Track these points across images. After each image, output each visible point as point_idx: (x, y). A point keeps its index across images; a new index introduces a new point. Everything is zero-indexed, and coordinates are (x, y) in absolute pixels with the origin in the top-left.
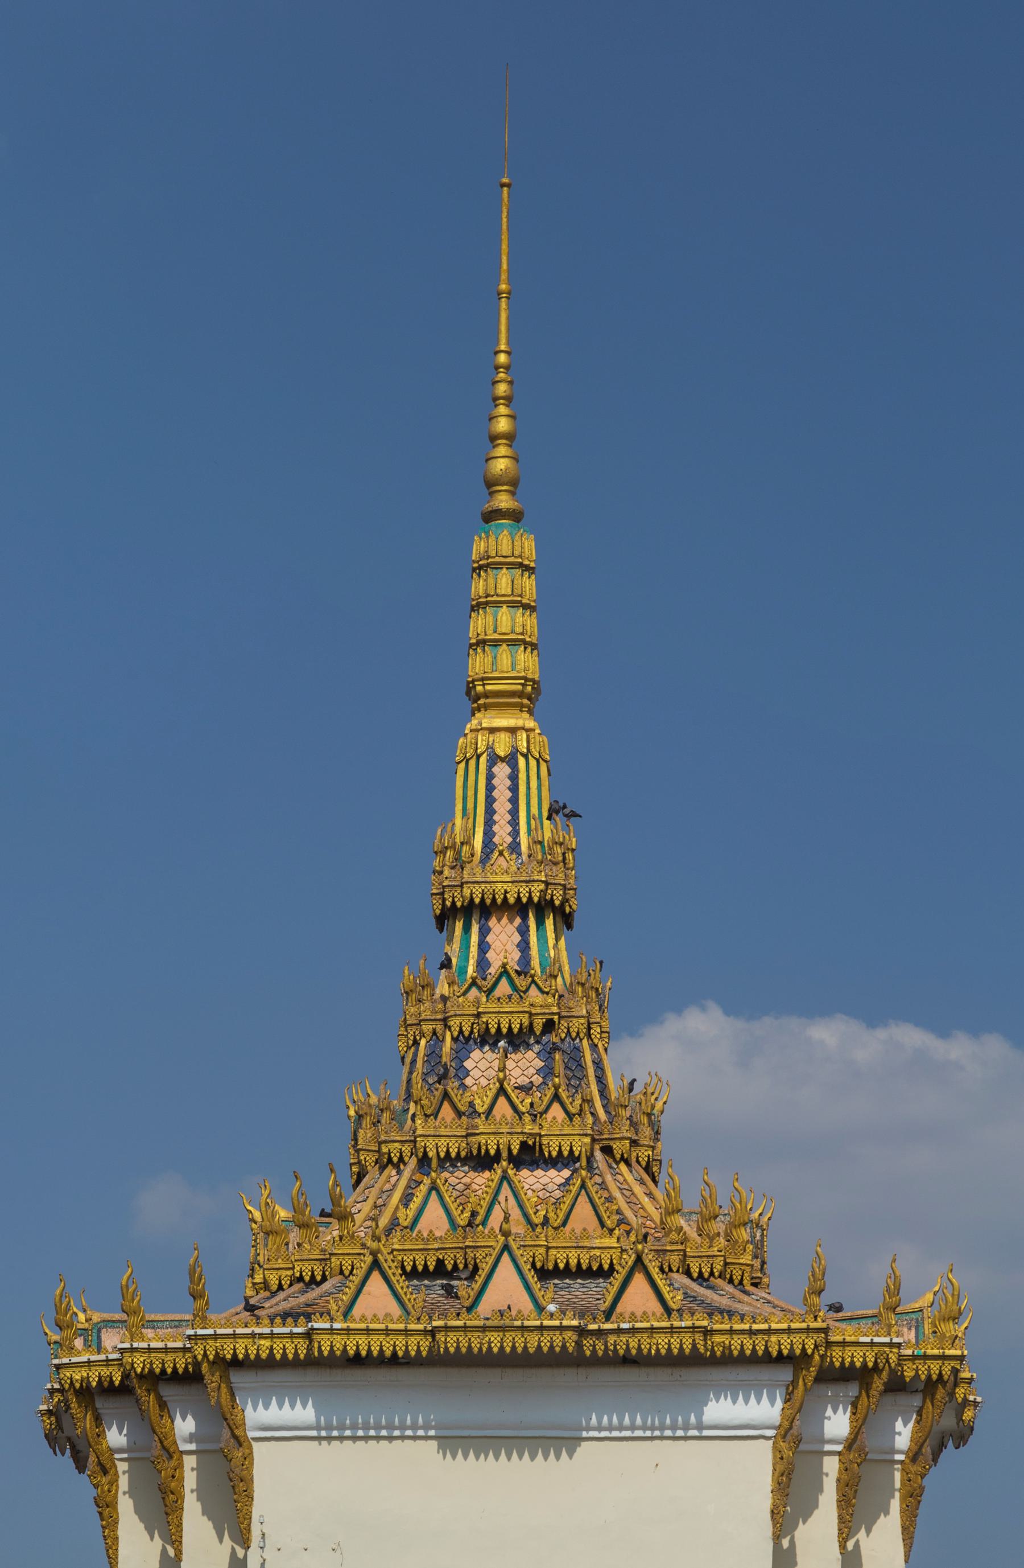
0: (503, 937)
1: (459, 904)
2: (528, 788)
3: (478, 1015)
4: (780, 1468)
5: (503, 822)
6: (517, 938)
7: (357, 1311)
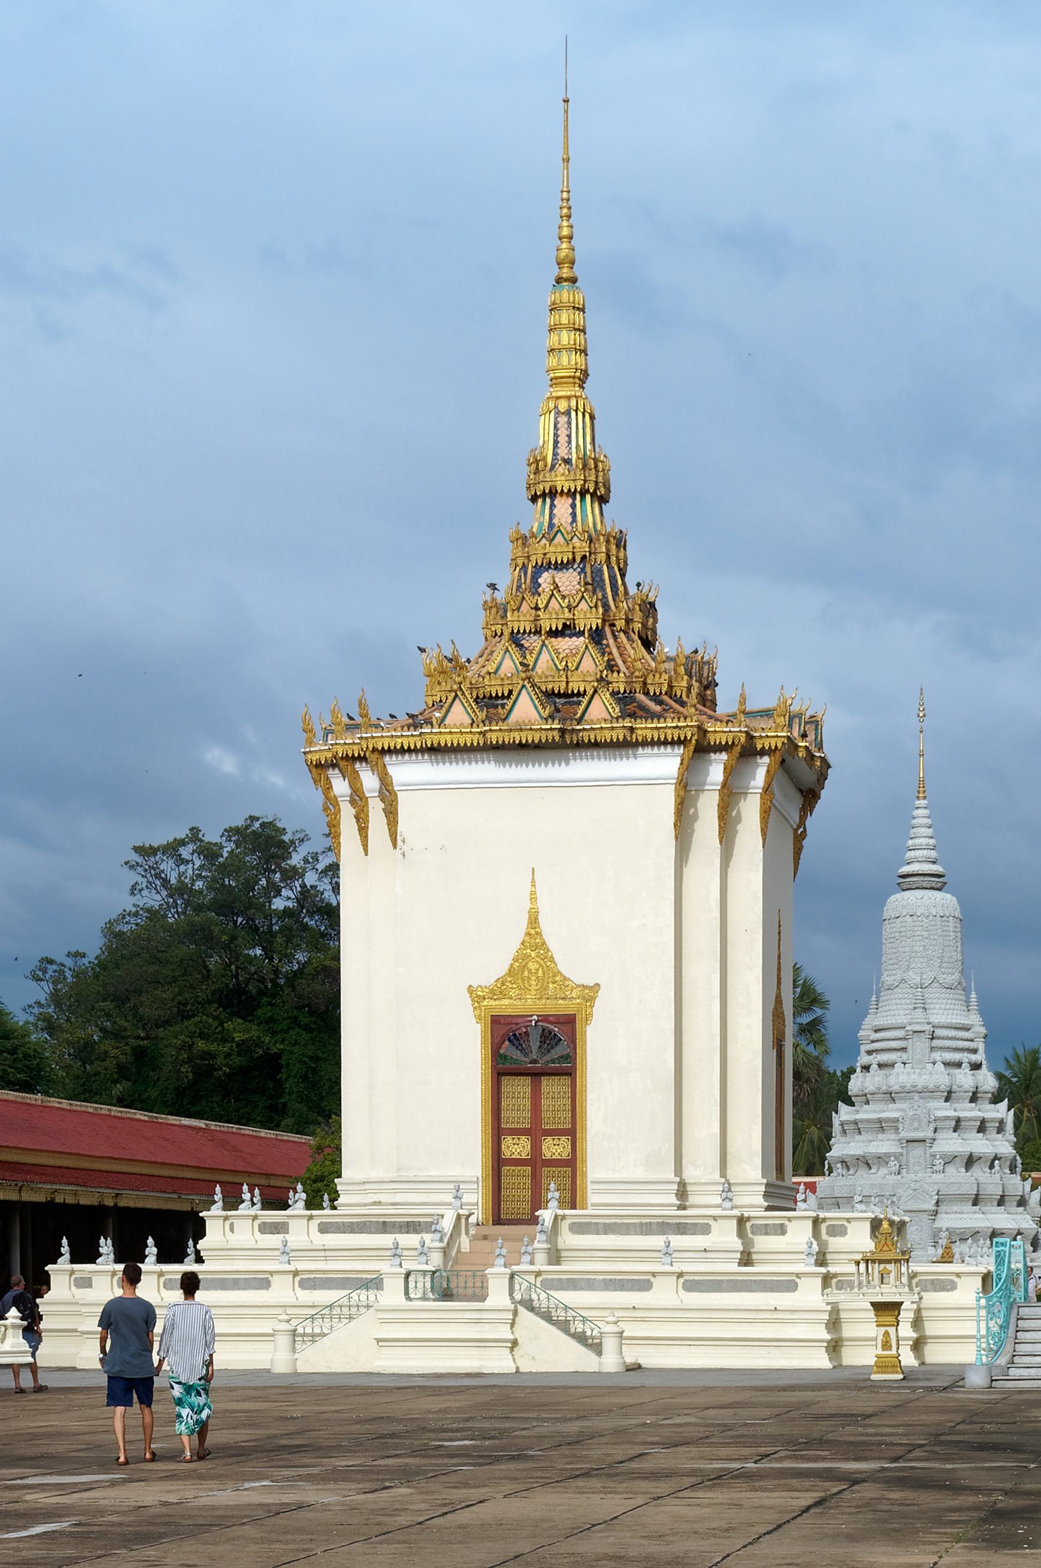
0: (563, 510)
1: (538, 493)
2: (577, 428)
3: (545, 554)
4: (679, 800)
5: (563, 448)
6: (571, 510)
7: (447, 722)
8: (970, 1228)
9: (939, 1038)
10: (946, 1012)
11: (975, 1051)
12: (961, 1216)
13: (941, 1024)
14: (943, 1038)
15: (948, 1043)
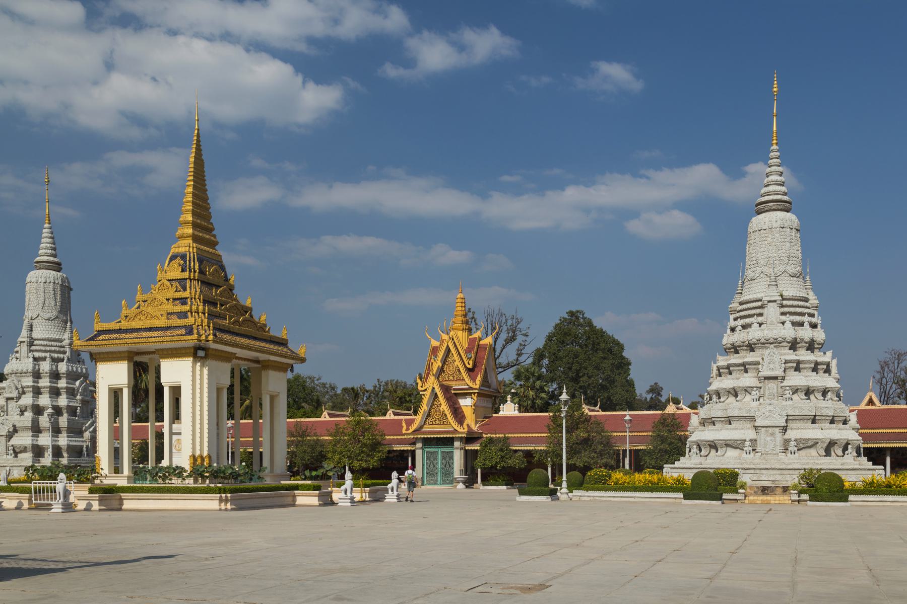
8: (22, 445)
9: (36, 345)
10: (44, 332)
11: (65, 353)
12: (21, 438)
13: (39, 338)
14: (39, 345)
15: (39, 348)
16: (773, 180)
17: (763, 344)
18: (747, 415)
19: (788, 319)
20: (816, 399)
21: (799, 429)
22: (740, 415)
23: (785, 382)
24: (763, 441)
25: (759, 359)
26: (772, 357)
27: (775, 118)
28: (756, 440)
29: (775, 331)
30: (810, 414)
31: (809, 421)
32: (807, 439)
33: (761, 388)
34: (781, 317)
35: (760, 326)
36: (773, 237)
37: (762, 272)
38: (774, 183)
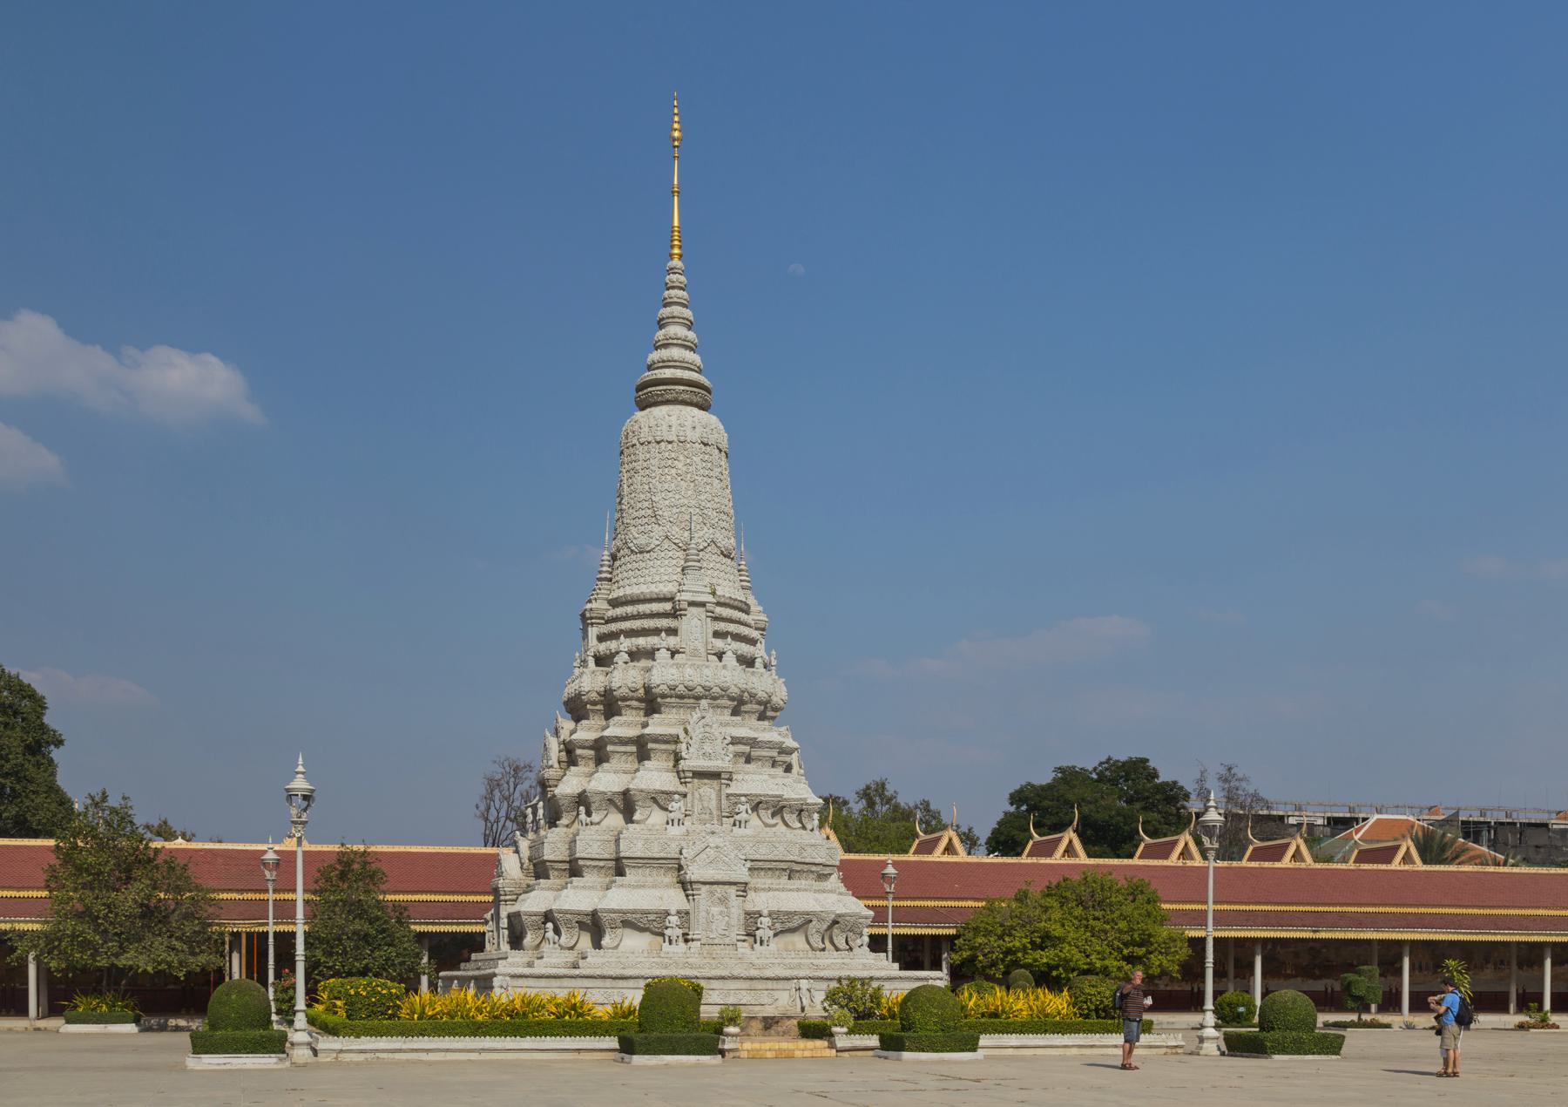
16: (679, 336)
17: (681, 697)
18: (662, 855)
19: (729, 647)
20: (785, 828)
21: (770, 889)
22: (646, 856)
23: (733, 784)
24: (704, 914)
25: (679, 731)
26: (707, 729)
27: (676, 198)
28: (687, 913)
29: (706, 671)
30: (788, 859)
31: (784, 873)
32: (790, 913)
33: (685, 796)
34: (714, 640)
35: (672, 657)
36: (688, 461)
37: (667, 537)
38: (680, 342)
